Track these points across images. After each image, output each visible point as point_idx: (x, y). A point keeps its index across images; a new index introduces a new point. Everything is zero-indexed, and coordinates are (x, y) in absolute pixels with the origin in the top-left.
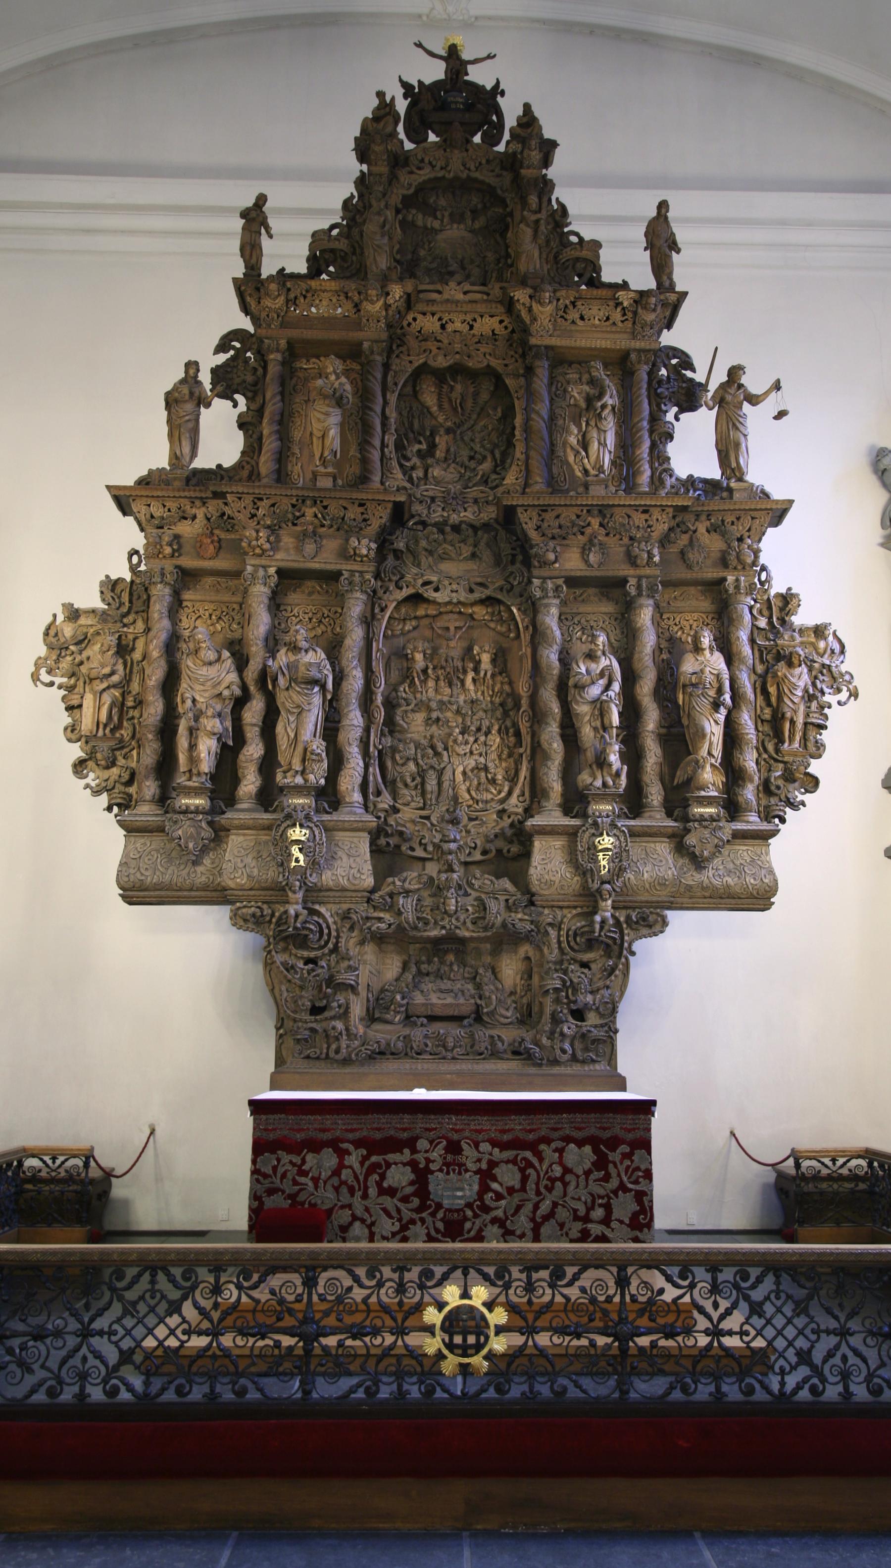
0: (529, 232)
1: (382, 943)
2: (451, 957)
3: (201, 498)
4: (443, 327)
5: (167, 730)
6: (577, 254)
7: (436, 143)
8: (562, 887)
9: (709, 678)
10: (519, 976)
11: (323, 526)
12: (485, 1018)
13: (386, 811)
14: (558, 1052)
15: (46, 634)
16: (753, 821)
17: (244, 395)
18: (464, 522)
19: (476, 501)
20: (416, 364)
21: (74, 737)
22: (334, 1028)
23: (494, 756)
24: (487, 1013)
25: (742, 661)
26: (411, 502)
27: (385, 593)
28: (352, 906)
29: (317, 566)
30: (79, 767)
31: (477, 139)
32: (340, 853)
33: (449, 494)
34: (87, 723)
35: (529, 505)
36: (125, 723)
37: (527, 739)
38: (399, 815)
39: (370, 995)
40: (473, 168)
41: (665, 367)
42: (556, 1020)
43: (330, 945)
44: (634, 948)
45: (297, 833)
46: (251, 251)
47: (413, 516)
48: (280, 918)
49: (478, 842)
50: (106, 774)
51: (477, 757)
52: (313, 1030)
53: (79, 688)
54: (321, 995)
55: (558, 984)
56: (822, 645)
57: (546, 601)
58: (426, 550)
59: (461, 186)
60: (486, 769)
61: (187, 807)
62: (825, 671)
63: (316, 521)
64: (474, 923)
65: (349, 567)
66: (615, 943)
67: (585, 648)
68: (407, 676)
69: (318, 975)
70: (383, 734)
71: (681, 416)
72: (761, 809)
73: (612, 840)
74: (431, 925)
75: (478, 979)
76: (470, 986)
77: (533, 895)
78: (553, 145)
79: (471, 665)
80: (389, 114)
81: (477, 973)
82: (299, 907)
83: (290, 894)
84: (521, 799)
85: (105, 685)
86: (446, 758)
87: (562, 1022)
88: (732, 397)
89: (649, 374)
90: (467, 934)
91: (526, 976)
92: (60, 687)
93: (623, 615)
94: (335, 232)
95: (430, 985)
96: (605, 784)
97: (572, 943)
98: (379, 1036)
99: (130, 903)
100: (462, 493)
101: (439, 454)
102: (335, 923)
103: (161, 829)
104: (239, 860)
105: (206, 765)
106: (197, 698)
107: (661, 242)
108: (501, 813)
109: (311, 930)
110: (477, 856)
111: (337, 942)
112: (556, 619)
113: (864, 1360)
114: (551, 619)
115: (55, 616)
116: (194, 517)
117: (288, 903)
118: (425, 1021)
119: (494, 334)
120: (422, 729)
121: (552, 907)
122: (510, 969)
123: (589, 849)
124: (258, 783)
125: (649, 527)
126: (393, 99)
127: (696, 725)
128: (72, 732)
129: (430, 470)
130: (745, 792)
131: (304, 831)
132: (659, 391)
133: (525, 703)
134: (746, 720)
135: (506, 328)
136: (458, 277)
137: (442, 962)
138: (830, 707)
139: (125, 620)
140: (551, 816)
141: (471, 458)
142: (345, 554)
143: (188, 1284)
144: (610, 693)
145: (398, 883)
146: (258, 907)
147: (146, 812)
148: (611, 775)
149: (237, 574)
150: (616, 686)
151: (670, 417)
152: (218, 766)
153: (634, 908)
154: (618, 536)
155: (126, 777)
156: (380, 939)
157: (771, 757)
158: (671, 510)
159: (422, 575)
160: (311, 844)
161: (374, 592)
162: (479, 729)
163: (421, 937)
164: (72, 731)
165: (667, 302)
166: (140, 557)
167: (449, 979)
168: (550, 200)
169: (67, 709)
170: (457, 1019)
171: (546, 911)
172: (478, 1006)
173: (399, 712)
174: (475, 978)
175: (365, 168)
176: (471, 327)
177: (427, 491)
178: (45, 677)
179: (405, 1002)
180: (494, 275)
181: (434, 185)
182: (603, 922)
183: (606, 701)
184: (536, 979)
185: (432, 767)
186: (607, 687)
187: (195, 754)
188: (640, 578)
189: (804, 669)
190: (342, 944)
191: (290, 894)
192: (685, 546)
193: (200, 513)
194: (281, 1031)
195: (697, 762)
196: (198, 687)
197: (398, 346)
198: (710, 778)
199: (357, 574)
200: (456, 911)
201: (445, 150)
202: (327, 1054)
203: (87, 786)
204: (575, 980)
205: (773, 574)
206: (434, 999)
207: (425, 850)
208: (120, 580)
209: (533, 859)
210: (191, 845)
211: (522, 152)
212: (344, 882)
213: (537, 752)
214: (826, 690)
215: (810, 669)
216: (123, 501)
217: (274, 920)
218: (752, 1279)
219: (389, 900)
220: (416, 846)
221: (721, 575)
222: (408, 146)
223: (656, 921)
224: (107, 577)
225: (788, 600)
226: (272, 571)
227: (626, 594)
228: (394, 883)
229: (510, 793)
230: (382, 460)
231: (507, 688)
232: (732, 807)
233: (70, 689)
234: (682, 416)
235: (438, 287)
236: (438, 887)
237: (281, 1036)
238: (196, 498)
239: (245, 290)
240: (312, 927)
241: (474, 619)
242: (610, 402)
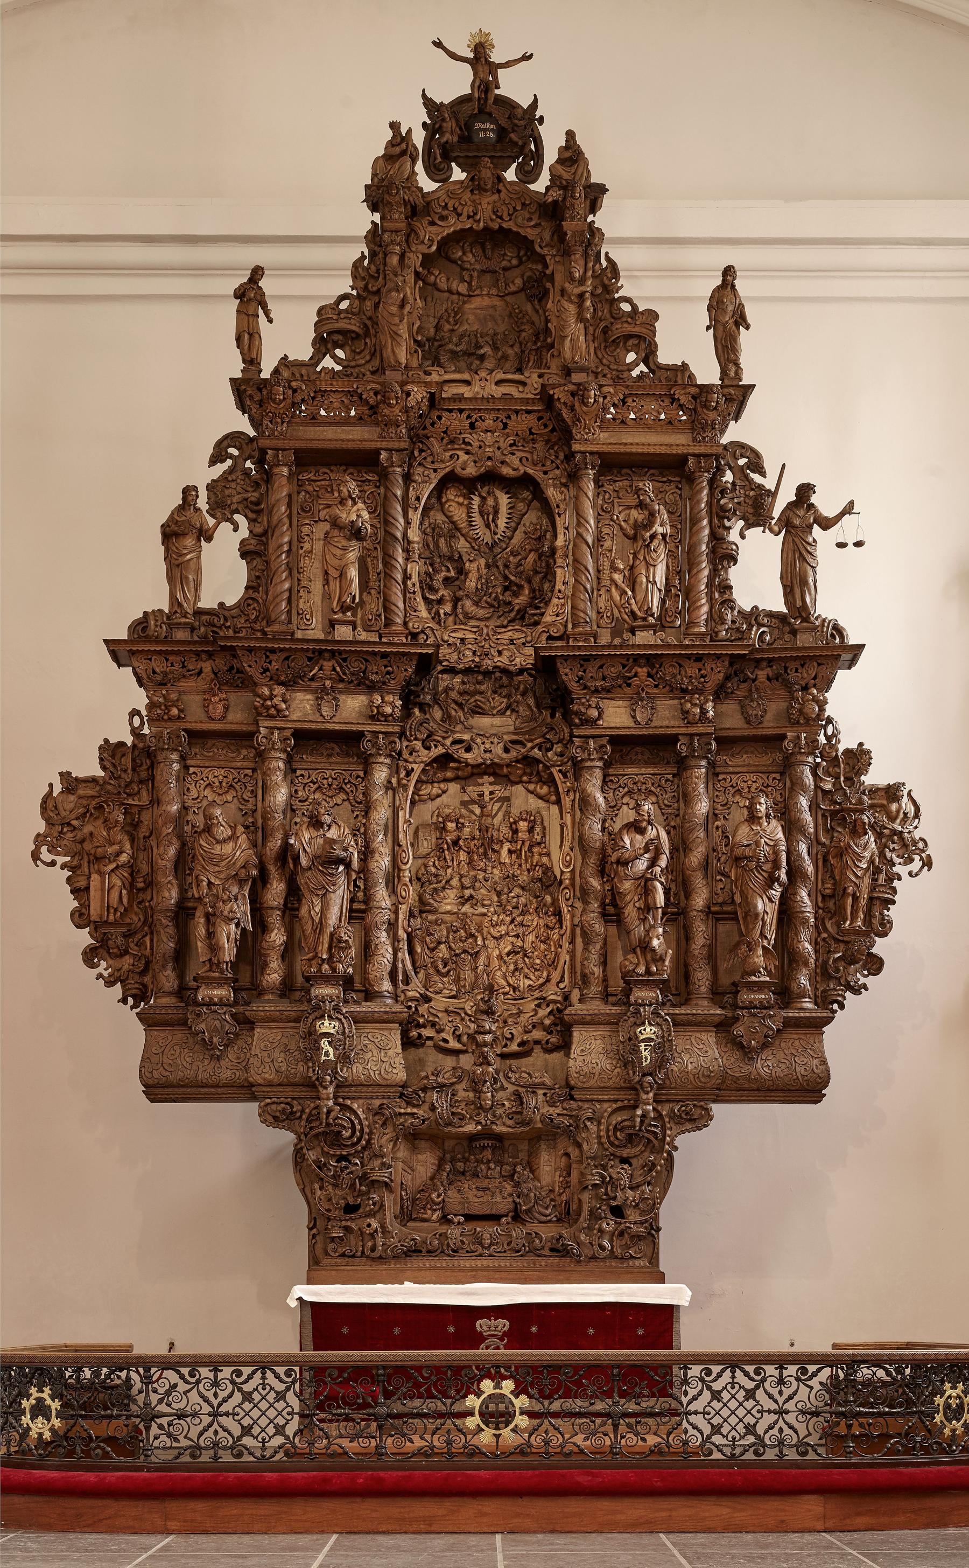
0: (572, 309)
2: (488, 1154)
4: (472, 426)
5: (183, 913)
6: (629, 329)
7: (462, 182)
11: (342, 680)
14: (596, 1248)
17: (246, 516)
18: (498, 667)
20: (441, 474)
25: (802, 830)
27: (411, 754)
28: (385, 1101)
29: (336, 727)
30: (90, 957)
31: (510, 175)
32: (370, 1046)
38: (432, 1004)
40: (506, 217)
41: (730, 468)
42: (594, 1216)
44: (676, 1143)
45: (327, 1026)
46: (248, 340)
48: (310, 1114)
50: (118, 963)
51: (514, 940)
52: (346, 1229)
56: (894, 807)
58: (456, 703)
59: (493, 238)
65: (372, 728)
69: (351, 1173)
71: (747, 533)
72: (819, 993)
73: (654, 1029)
78: (601, 189)
80: (404, 153)
81: (515, 1171)
82: (331, 1103)
85: (113, 866)
88: (801, 521)
89: (712, 482)
90: (504, 1129)
92: (62, 868)
94: (344, 305)
99: (152, 1101)
103: (183, 1023)
104: (268, 1052)
105: (228, 953)
107: (727, 317)
113: (796, 1431)
114: (593, 786)
115: (51, 785)
118: (462, 1219)
119: (531, 433)
123: (630, 1039)
125: (703, 676)
126: (410, 131)
128: (80, 918)
132: (722, 502)
135: (546, 426)
136: (489, 364)
138: (899, 879)
141: (506, 589)
143: (290, 1380)
146: (287, 1103)
150: (663, 862)
151: (734, 536)
152: (238, 955)
155: (141, 966)
156: (413, 1137)
157: (831, 936)
163: (456, 1133)
165: (735, 395)
168: (599, 253)
169: (72, 892)
171: (586, 1105)
174: (513, 1175)
175: (377, 217)
176: (505, 426)
178: (46, 856)
180: (532, 358)
181: (459, 237)
182: (644, 1116)
184: (575, 1174)
186: (653, 863)
187: (213, 942)
188: (692, 735)
190: (375, 1142)
194: (315, 1231)
197: (421, 451)
199: (381, 736)
201: (472, 191)
202: (363, 1252)
203: (100, 976)
205: (839, 727)
208: (122, 744)
211: (564, 199)
215: (879, 836)
216: (118, 651)
218: (714, 1375)
220: (450, 1039)
222: (427, 184)
224: (106, 741)
225: (859, 759)
226: (288, 733)
232: (785, 994)
234: (747, 533)
235: (466, 376)
237: (314, 1236)
239: (245, 391)
242: (660, 530)
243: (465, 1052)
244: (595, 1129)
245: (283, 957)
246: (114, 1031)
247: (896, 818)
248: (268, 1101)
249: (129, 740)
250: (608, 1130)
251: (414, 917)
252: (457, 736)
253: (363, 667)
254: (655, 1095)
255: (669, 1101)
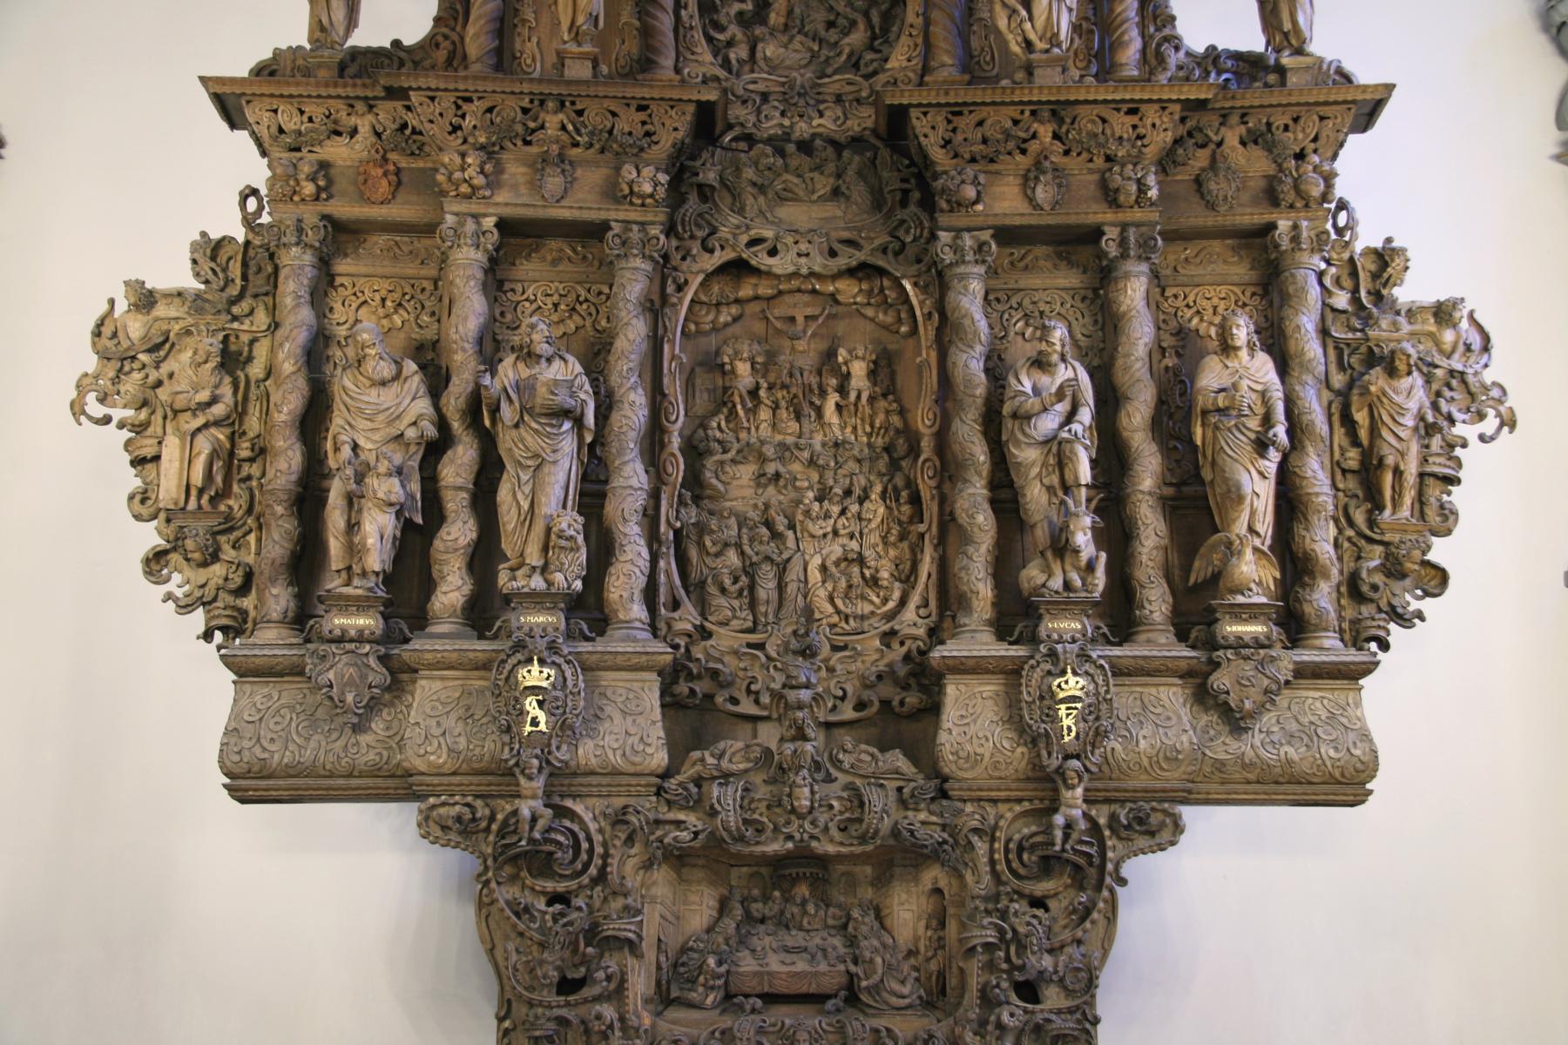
1: (684, 866)
2: (803, 890)
3: (366, 98)
5: (308, 499)
8: (996, 765)
9: (1247, 398)
10: (923, 923)
11: (576, 145)
12: (864, 997)
13: (690, 636)
15: (97, 333)
16: (1329, 647)
18: (820, 135)
19: (839, 99)
21: (145, 511)
22: (599, 1017)
23: (874, 538)
24: (867, 988)
25: (1306, 367)
26: (727, 103)
27: (684, 259)
28: (631, 801)
30: (155, 563)
32: (608, 709)
33: (792, 88)
34: (169, 488)
35: (929, 105)
36: (236, 488)
37: (931, 508)
39: (663, 959)
42: (988, 1000)
43: (593, 871)
47: (730, 127)
48: (505, 823)
49: (849, 688)
50: (201, 575)
51: (845, 540)
52: (562, 1022)
53: (156, 428)
54: (577, 959)
55: (991, 936)
56: (1448, 336)
57: (961, 269)
58: (754, 184)
60: (861, 560)
61: (344, 631)
62: (1454, 383)
63: (565, 137)
64: (843, 830)
65: (622, 216)
66: (1091, 864)
67: (1031, 349)
68: (723, 400)
69: (571, 923)
70: (682, 502)
72: (1346, 626)
73: (1082, 682)
74: (769, 833)
75: (850, 929)
76: (837, 941)
77: (945, 779)
79: (834, 382)
81: (849, 917)
82: (538, 804)
83: (522, 781)
84: (922, 612)
85: (200, 421)
86: (791, 543)
87: (1000, 1004)
90: (831, 849)
91: (934, 923)
92: (121, 426)
93: (1095, 290)
95: (767, 939)
96: (1067, 585)
97: (1015, 864)
98: (678, 1030)
99: (243, 801)
100: (815, 85)
101: (775, 18)
102: (601, 831)
103: (297, 671)
104: (434, 721)
105: (377, 557)
106: (361, 442)
108: (888, 636)
109: (558, 843)
110: (848, 713)
111: (605, 865)
112: (979, 300)
114: (970, 299)
115: (112, 302)
116: (354, 132)
117: (519, 796)
118: (759, 1003)
120: (749, 492)
121: (980, 800)
122: (907, 910)
123: (1042, 698)
124: (467, 589)
125: (1139, 137)
127: (1226, 480)
128: (143, 503)
129: (760, 46)
130: (1316, 596)
131: (546, 671)
133: (927, 445)
134: (1315, 472)
137: (787, 899)
139: (236, 310)
140: (976, 640)
141: (831, 25)
142: (614, 193)
144: (1076, 427)
145: (710, 760)
146: (467, 805)
147: (271, 640)
148: (1078, 569)
149: (429, 229)
150: (1086, 415)
152: (398, 559)
153: (1123, 802)
154: (1085, 155)
155: (237, 580)
156: (678, 859)
157: (1361, 534)
158: (1177, 108)
159: (748, 228)
160: (559, 694)
161: (666, 257)
162: (848, 492)
163: (751, 854)
164: (143, 502)
166: (260, 200)
167: (801, 929)
169: (134, 463)
170: (815, 999)
171: (969, 808)
172: (851, 975)
173: (710, 463)
174: (845, 927)
177: (755, 82)
178: (95, 408)
179: (723, 969)
182: (1069, 826)
183: (1068, 441)
184: (952, 927)
185: (768, 558)
186: (1070, 417)
187: (357, 540)
188: (1124, 227)
189: (1417, 379)
191: (522, 781)
192: (1203, 170)
193: (364, 124)
194: (507, 1024)
195: (1229, 544)
196: (362, 424)
199: (635, 228)
200: (812, 808)
203: (169, 597)
204: (1022, 930)
205: (1358, 215)
206: (774, 964)
207: (757, 702)
209: (944, 717)
210: (350, 698)
212: (617, 760)
213: (950, 529)
214: (1458, 416)
215: (1429, 379)
216: (230, 103)
217: (494, 827)
219: (694, 790)
220: (742, 696)
221: (1267, 218)
223: (1163, 825)
224: (204, 234)
225: (1386, 259)
226: (489, 223)
227: (1102, 255)
228: (703, 760)
229: (903, 602)
230: (676, 31)
231: (896, 420)
232: (1293, 623)
233: (140, 428)
236: (781, 768)
237: (506, 1032)
238: (357, 98)
240: (561, 838)
241: (837, 302)
243: (767, 718)
244: (986, 846)
245: (471, 566)
246: (185, 687)
247: (1453, 352)
248: (432, 800)
249: (240, 234)
250: (1007, 850)
251: (686, 505)
252: (752, 232)
253: (609, 126)
254: (1086, 790)
255: (1108, 801)
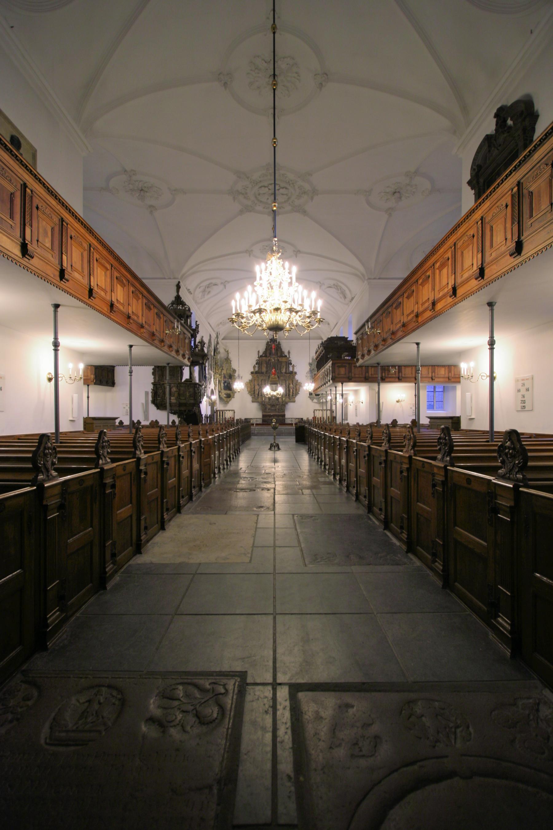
46: (258, 354)
104: (260, 400)
107: (289, 353)
122: (278, 407)
198: (291, 394)
